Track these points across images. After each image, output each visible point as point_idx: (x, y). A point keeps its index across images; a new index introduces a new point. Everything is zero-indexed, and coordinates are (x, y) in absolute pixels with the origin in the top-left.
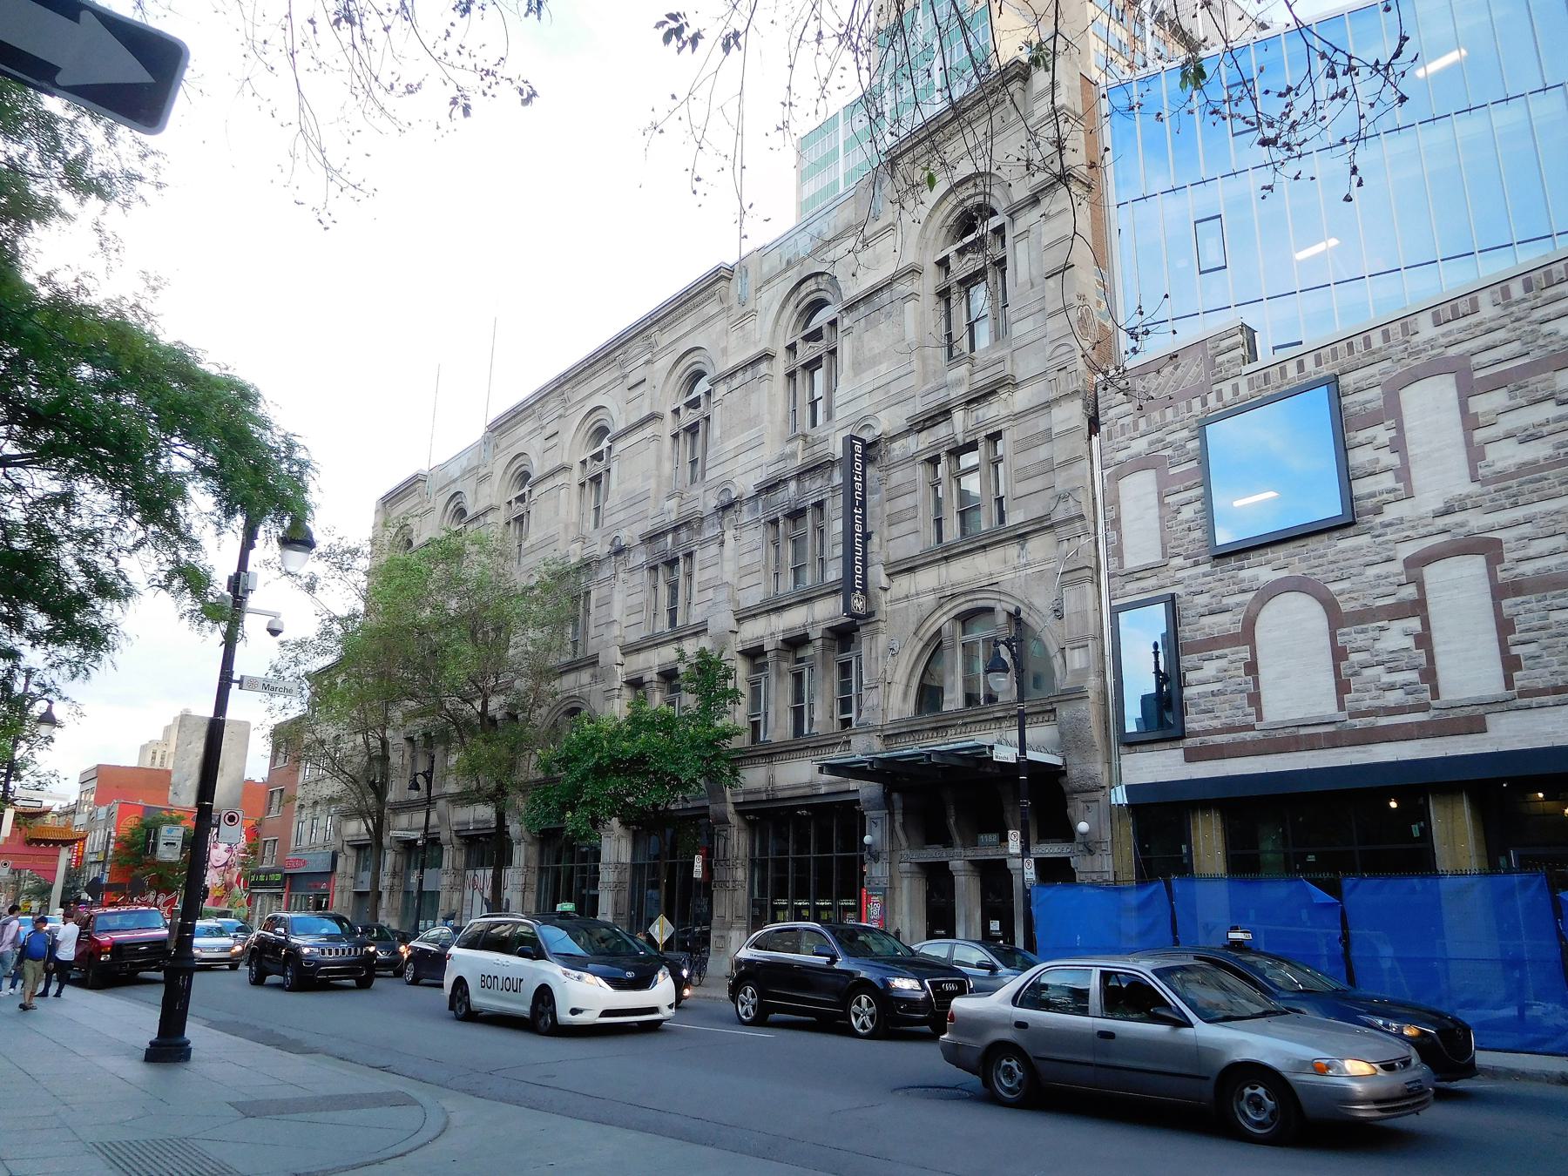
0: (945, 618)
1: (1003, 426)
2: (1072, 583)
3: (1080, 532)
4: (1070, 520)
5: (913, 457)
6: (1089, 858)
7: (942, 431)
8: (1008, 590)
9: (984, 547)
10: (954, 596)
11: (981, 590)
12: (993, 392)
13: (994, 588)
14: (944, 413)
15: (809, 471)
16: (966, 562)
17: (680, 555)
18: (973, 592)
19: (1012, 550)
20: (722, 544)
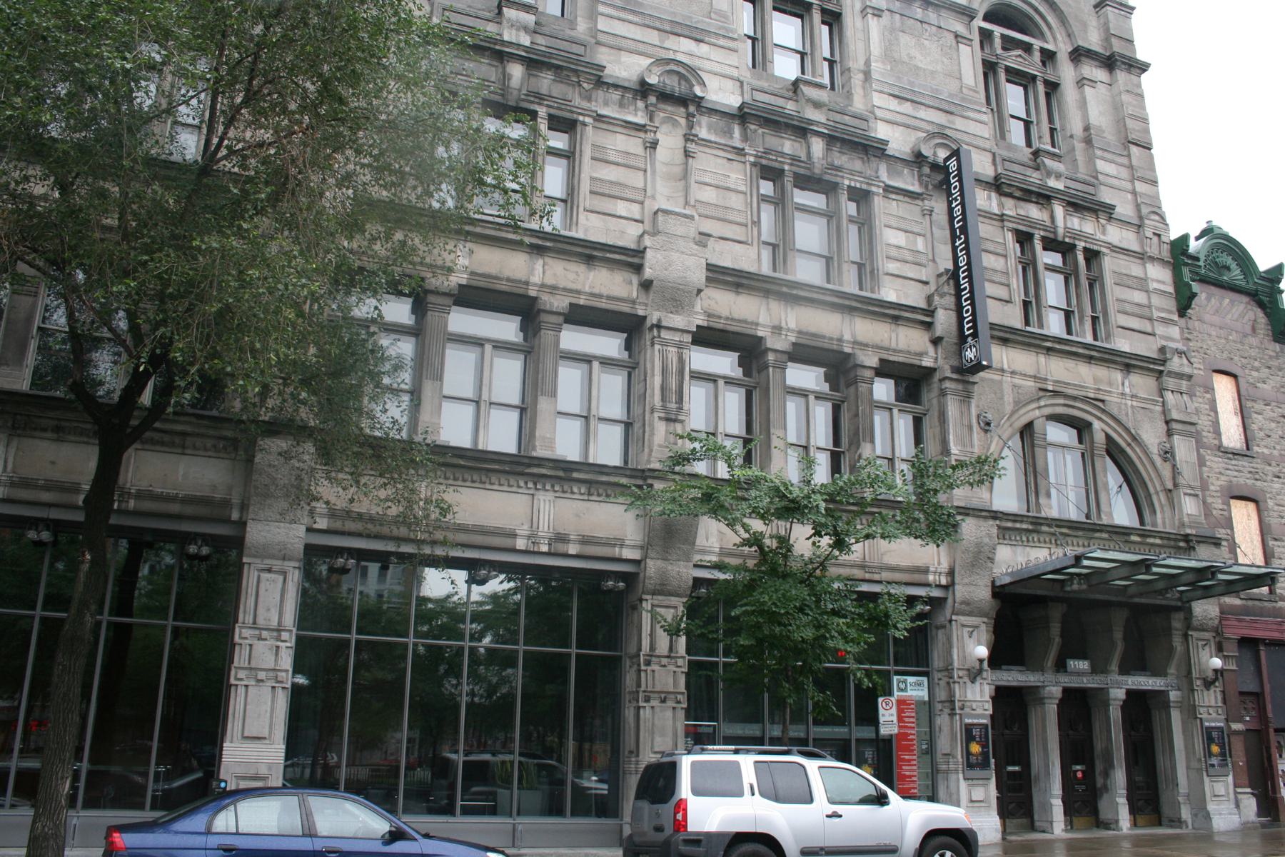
0: (1037, 413)
1: (1104, 250)
2: (1184, 434)
3: (1184, 389)
4: (1180, 376)
5: (1002, 218)
6: (1206, 693)
7: (1034, 212)
8: (1115, 412)
9: (1091, 358)
10: (1056, 393)
11: (1085, 400)
12: (1095, 211)
13: (1100, 404)
14: (1044, 198)
15: (843, 141)
16: (1070, 363)
17: (542, 112)
18: (1075, 398)
19: (1118, 376)
20: (654, 145)
